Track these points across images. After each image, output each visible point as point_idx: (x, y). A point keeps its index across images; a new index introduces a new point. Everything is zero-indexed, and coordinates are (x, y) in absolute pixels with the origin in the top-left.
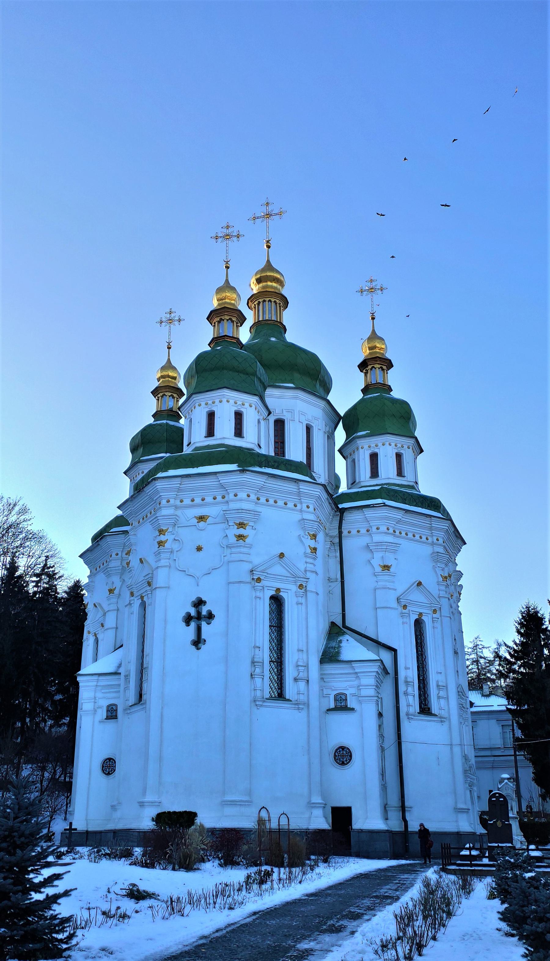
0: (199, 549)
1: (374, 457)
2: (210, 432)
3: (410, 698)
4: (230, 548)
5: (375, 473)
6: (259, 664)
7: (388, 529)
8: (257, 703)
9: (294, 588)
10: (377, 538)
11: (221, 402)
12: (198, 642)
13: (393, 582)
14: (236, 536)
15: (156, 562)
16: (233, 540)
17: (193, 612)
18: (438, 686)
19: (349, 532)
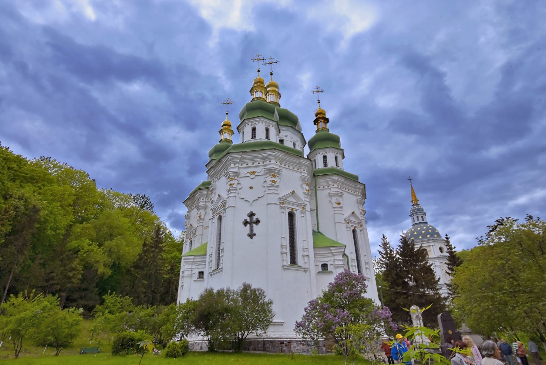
0: (251, 188)
1: (325, 157)
2: (254, 136)
3: (354, 268)
4: (268, 187)
5: (325, 164)
6: (285, 246)
7: (338, 186)
8: (285, 267)
9: (300, 209)
10: (333, 190)
11: (259, 123)
12: (252, 235)
13: (342, 211)
14: (270, 181)
15: (228, 194)
16: (269, 183)
17: (248, 219)
18: (365, 262)
19: (319, 188)
